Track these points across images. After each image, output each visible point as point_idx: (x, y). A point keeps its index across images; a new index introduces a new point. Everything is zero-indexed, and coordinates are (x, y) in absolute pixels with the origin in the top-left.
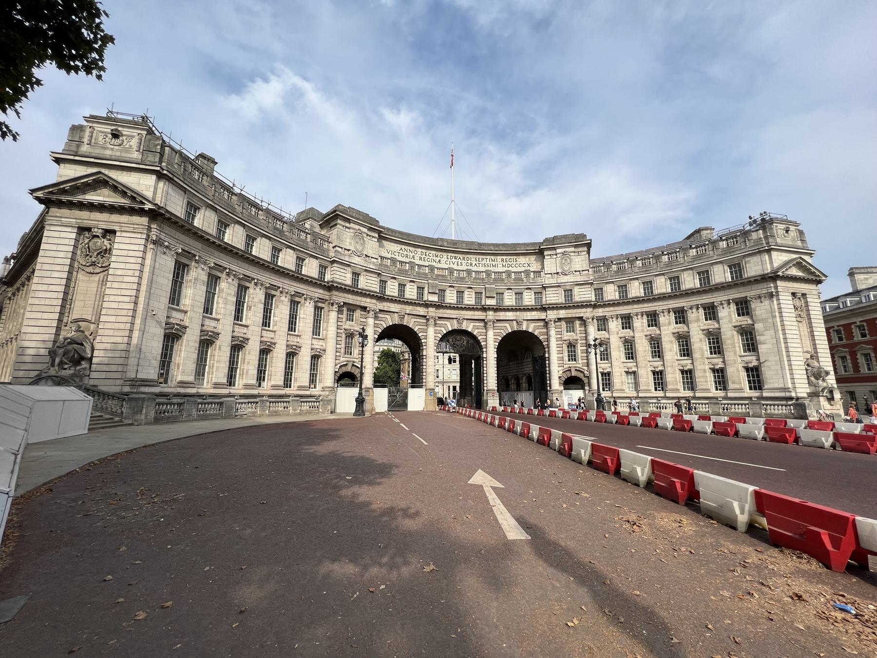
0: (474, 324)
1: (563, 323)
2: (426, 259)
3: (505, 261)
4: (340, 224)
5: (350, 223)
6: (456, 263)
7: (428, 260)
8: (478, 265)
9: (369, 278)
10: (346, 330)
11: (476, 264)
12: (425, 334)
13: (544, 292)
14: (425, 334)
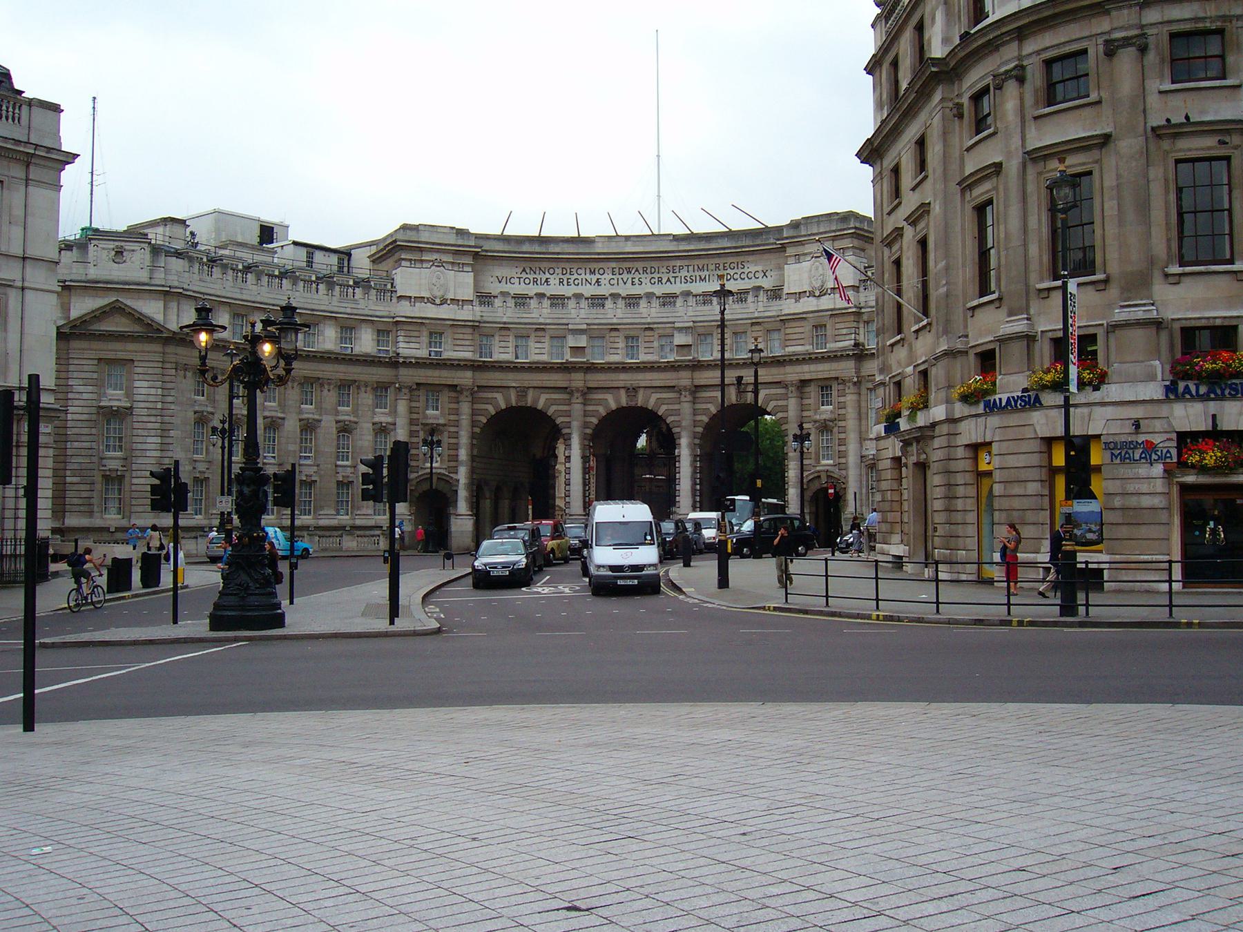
0: (659, 396)
1: (812, 390)
2: (571, 281)
3: (721, 267)
4: (403, 259)
5: (422, 251)
6: (630, 279)
7: (576, 282)
8: (672, 280)
9: (457, 336)
10: (425, 425)
11: (668, 280)
12: (567, 419)
13: (782, 330)
14: (567, 419)
